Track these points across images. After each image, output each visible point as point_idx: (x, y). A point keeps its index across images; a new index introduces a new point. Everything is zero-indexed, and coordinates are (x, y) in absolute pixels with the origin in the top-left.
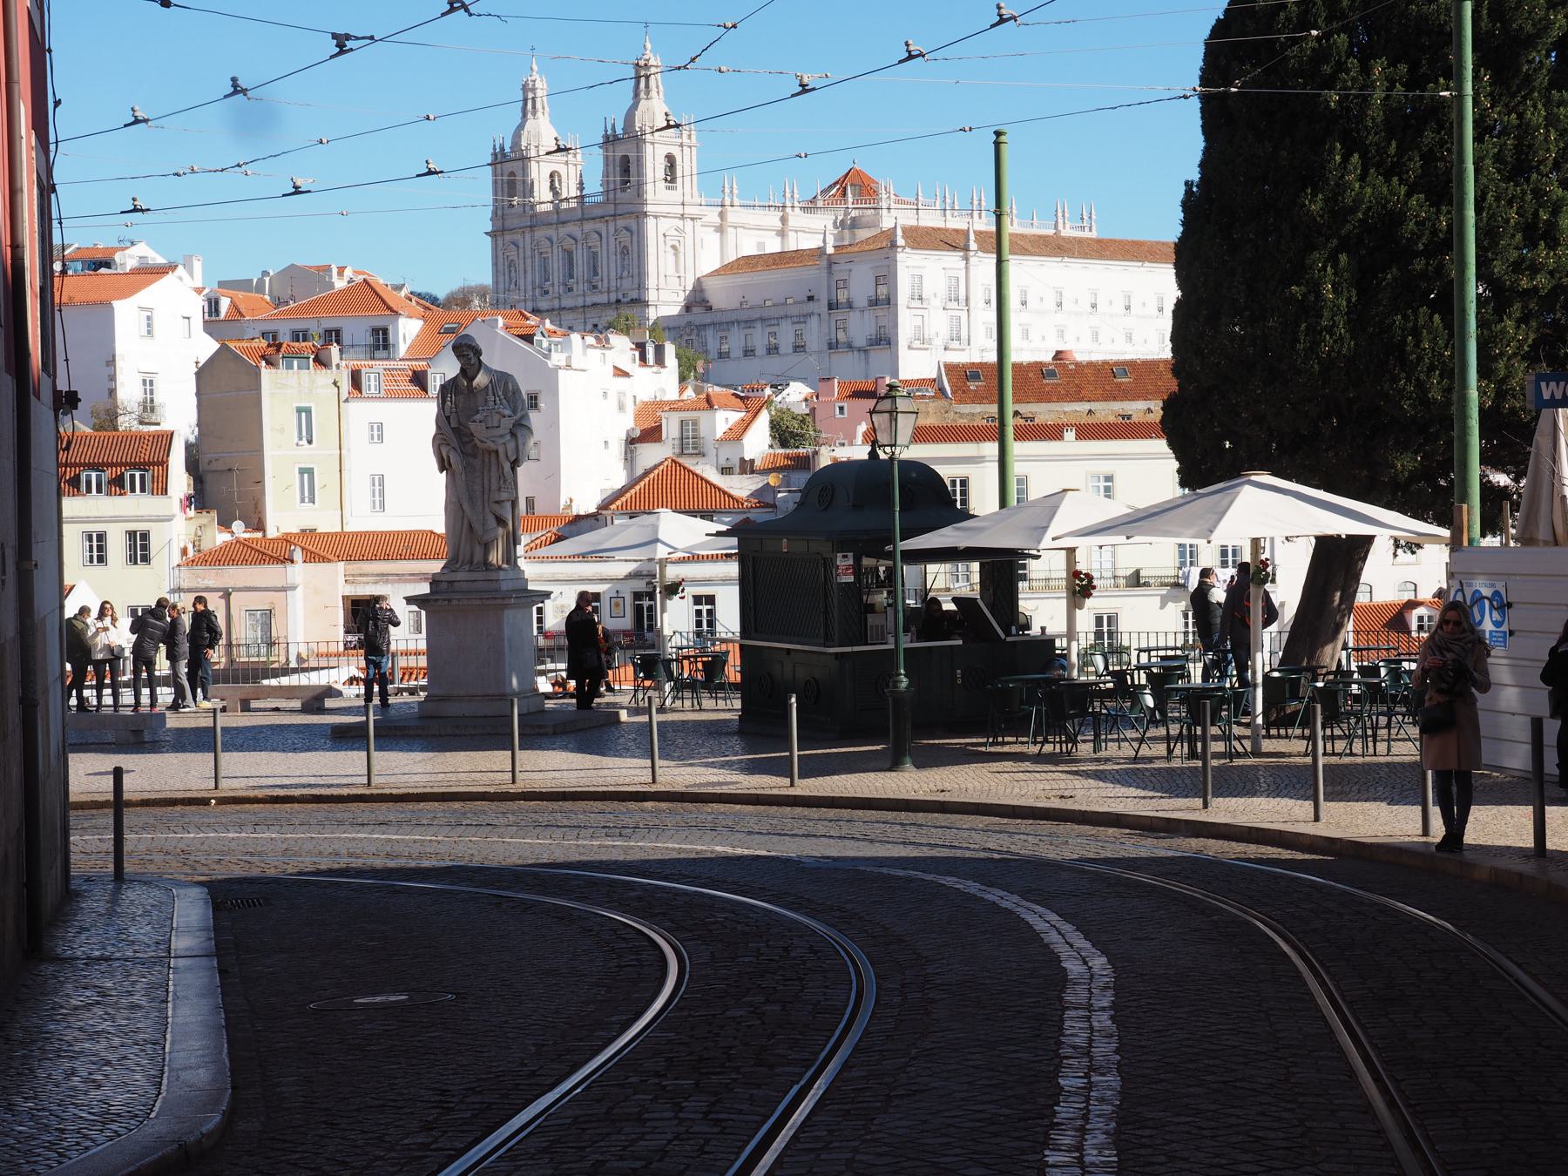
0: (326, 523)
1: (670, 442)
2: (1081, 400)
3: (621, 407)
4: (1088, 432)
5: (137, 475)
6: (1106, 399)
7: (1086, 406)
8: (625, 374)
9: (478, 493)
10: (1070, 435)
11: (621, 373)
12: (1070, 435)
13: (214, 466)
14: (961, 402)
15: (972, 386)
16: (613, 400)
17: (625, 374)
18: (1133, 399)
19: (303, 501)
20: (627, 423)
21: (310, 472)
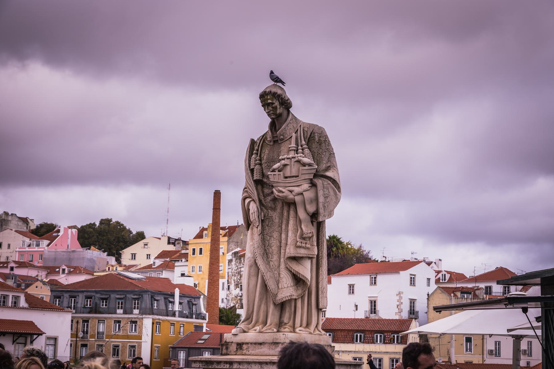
9: (274, 248)
19: (467, 351)
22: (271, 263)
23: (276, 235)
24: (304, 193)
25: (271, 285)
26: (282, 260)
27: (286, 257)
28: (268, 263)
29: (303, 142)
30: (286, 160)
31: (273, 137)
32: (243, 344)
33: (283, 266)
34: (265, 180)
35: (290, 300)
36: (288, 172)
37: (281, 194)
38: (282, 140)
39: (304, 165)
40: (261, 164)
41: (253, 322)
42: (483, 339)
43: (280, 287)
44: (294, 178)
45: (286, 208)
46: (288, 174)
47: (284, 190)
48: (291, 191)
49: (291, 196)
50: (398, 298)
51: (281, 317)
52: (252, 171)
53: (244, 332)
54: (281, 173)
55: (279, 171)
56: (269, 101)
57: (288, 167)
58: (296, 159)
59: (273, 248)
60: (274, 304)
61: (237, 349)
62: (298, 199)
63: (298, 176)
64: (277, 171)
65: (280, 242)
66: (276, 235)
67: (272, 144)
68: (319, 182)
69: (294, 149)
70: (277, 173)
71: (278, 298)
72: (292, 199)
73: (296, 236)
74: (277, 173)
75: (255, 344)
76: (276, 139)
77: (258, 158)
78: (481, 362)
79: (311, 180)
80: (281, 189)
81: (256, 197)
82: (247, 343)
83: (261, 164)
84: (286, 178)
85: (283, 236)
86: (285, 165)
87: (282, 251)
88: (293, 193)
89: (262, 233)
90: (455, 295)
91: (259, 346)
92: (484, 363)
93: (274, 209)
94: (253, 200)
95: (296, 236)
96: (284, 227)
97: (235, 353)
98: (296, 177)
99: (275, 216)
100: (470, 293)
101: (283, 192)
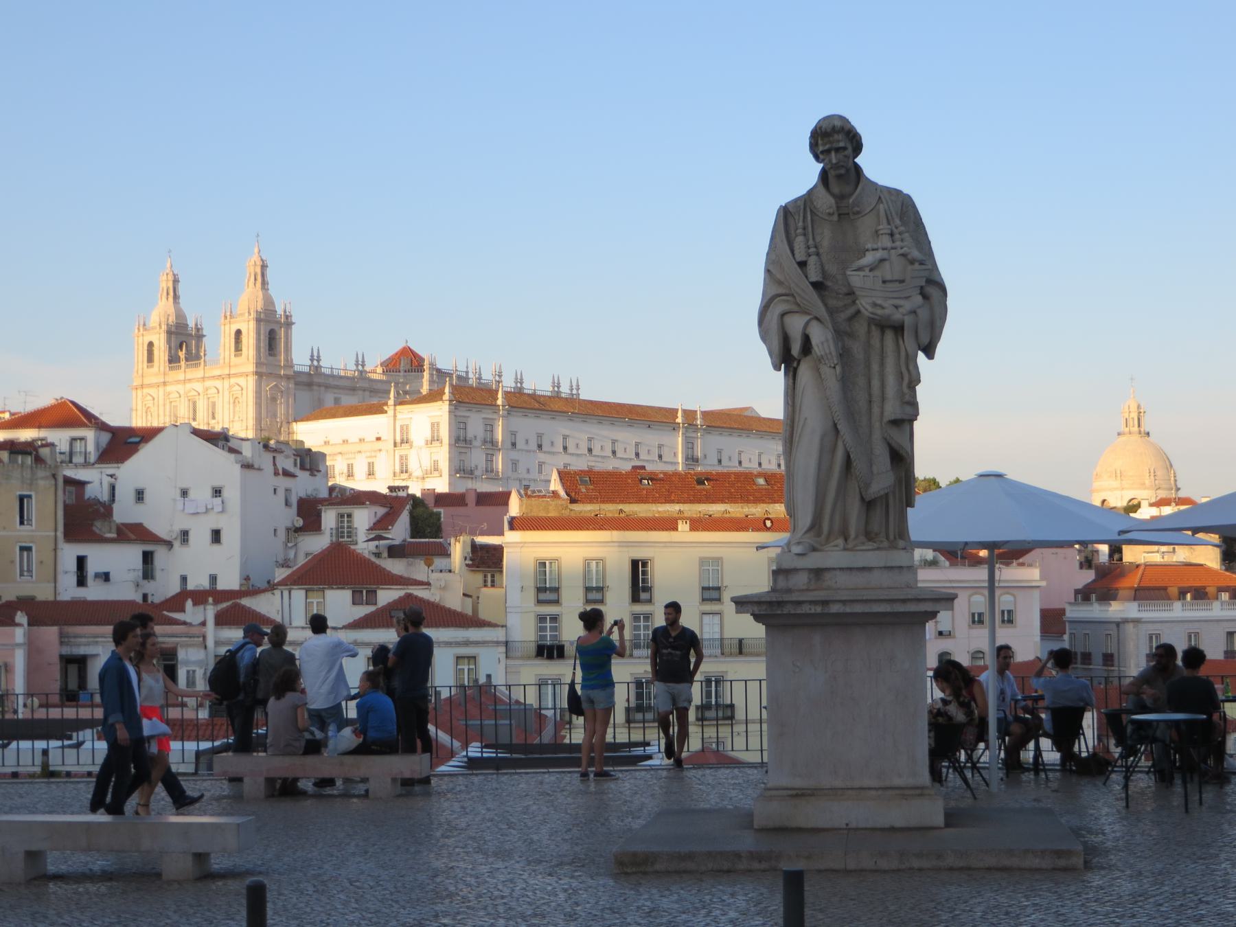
0: (43, 593)
1: (328, 532)
2: (672, 502)
3: (287, 504)
4: (698, 524)
6: (691, 502)
7: (676, 507)
8: (293, 476)
10: (683, 526)
11: (286, 474)
12: (683, 526)
16: (281, 493)
17: (293, 476)
18: (713, 502)
19: (21, 575)
20: (291, 517)
21: (29, 549)
23: (861, 381)
24: (919, 311)
25: (859, 465)
26: (877, 425)
27: (886, 419)
29: (898, 222)
31: (838, 207)
33: (877, 436)
34: (829, 283)
35: (881, 497)
36: (886, 272)
37: (879, 312)
38: (858, 213)
39: (912, 262)
40: (818, 254)
42: (55, 550)
43: (875, 471)
44: (897, 284)
45: (876, 333)
46: (888, 277)
47: (885, 305)
48: (896, 307)
49: (897, 316)
51: (867, 523)
52: (802, 264)
53: (814, 549)
54: (877, 273)
55: (871, 270)
56: (842, 144)
57: (887, 264)
58: (901, 251)
60: (862, 499)
61: (810, 580)
62: (908, 321)
64: (867, 270)
65: (870, 395)
66: (861, 381)
67: (835, 218)
68: (931, 290)
70: (867, 272)
73: (901, 384)
74: (867, 272)
75: (851, 569)
77: (811, 242)
78: (51, 598)
79: (922, 288)
80: (879, 302)
81: (822, 311)
82: (834, 569)
83: (818, 254)
84: (884, 282)
85: (876, 383)
86: (882, 260)
87: (876, 410)
88: (901, 310)
89: (846, 382)
92: (59, 598)
93: (851, 335)
94: (817, 319)
95: (901, 384)
96: (875, 367)
98: (902, 281)
99: (857, 349)
100: (30, 454)
101: (883, 308)
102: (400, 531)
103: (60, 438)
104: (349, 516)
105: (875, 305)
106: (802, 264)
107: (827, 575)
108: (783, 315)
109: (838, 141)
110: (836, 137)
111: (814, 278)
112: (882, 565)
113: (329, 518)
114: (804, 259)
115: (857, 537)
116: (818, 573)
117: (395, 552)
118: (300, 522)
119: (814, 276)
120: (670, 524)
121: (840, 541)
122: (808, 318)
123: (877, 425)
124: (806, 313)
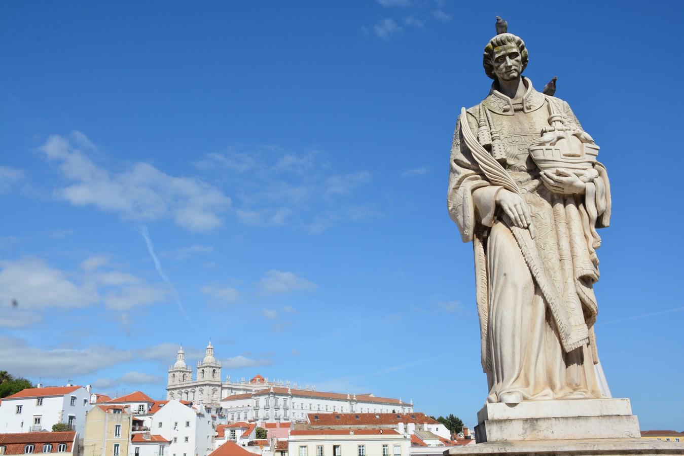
2: (347, 424)
4: (357, 432)
5: (62, 445)
6: (354, 424)
7: (349, 426)
10: (352, 433)
12: (352, 433)
13: (88, 444)
14: (314, 424)
15: (316, 420)
16: (211, 423)
22: (557, 285)
27: (579, 275)
28: (553, 285)
30: (556, 131)
32: (537, 419)
34: (510, 161)
41: (532, 382)
43: (573, 323)
48: (578, 175)
49: (579, 182)
50: (60, 415)
53: (525, 399)
56: (515, 50)
58: (573, 132)
59: (553, 261)
62: (590, 187)
63: (579, 156)
69: (559, 118)
70: (548, 146)
71: (570, 342)
72: (580, 188)
75: (566, 418)
76: (520, 106)
88: (581, 177)
90: (109, 412)
91: (575, 422)
97: (521, 438)
102: (253, 437)
103: (134, 407)
104: (234, 431)
105: (559, 174)
106: (488, 148)
107: (542, 425)
108: (473, 191)
109: (512, 48)
110: (509, 44)
111: (498, 158)
112: (598, 414)
113: (227, 433)
114: (488, 142)
115: (562, 388)
116: (532, 422)
117: (251, 444)
118: (217, 434)
119: (499, 154)
120: (347, 432)
121: (548, 390)
122: (498, 187)
123: (570, 280)
124: (492, 183)
